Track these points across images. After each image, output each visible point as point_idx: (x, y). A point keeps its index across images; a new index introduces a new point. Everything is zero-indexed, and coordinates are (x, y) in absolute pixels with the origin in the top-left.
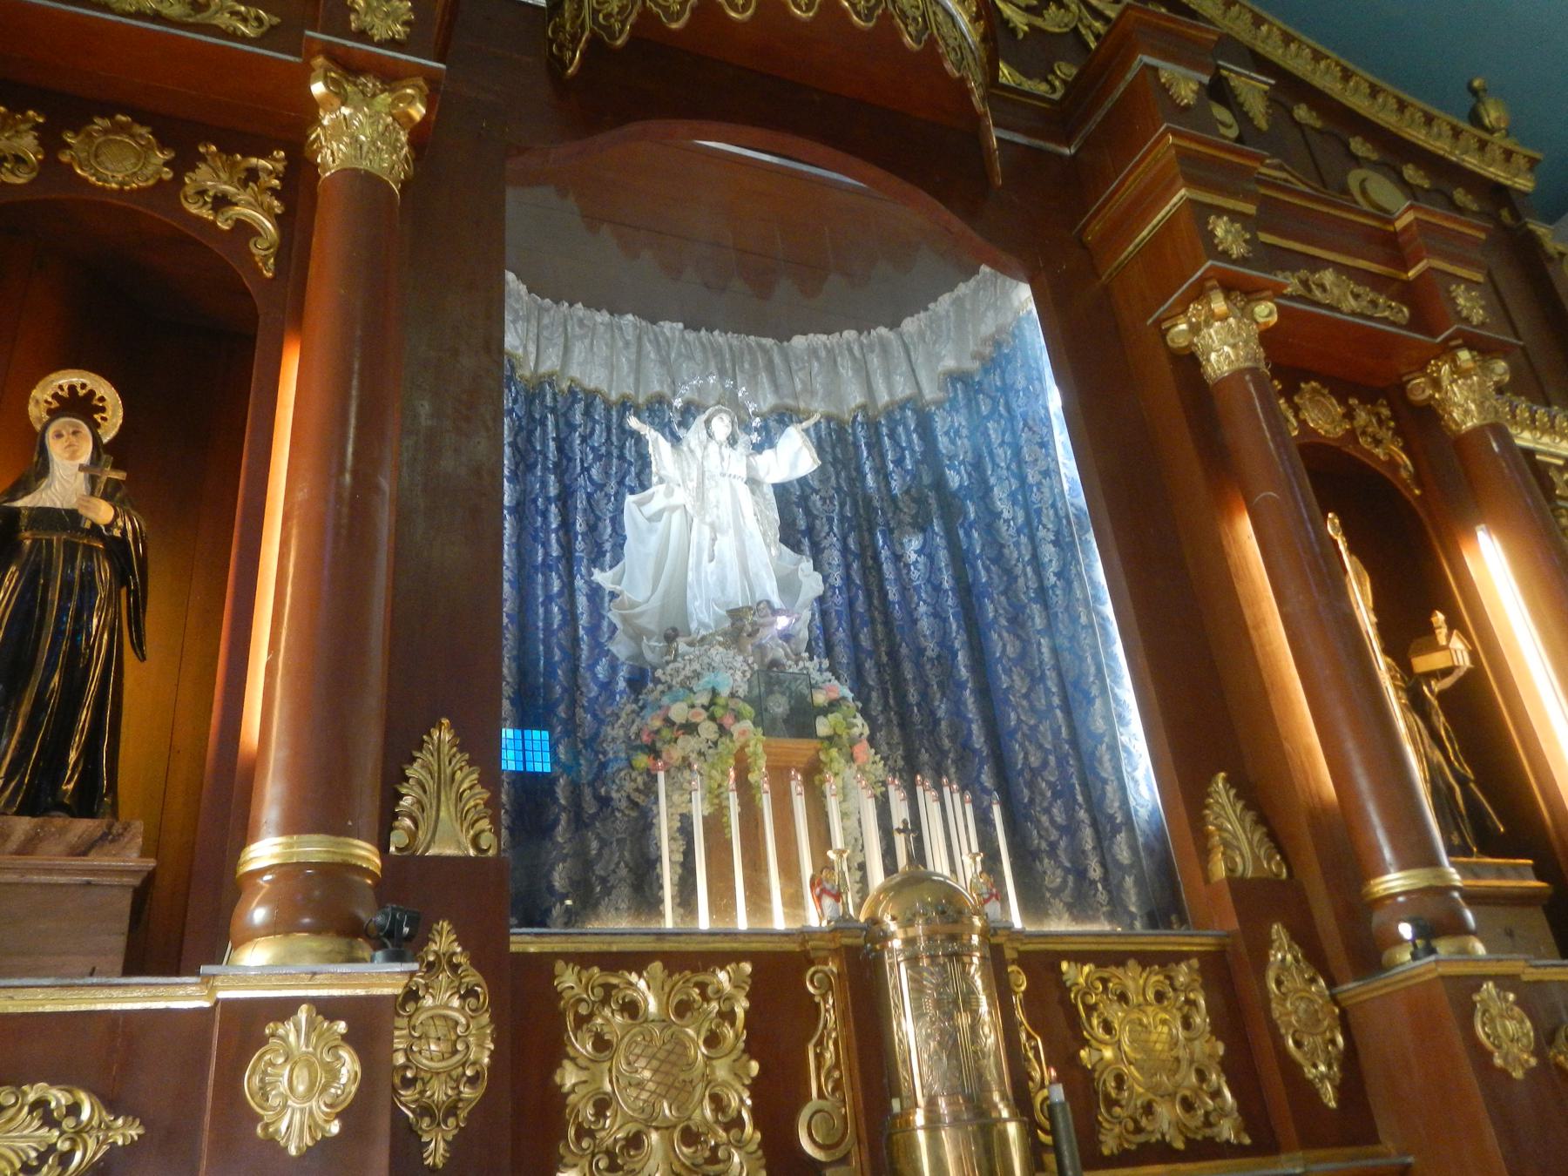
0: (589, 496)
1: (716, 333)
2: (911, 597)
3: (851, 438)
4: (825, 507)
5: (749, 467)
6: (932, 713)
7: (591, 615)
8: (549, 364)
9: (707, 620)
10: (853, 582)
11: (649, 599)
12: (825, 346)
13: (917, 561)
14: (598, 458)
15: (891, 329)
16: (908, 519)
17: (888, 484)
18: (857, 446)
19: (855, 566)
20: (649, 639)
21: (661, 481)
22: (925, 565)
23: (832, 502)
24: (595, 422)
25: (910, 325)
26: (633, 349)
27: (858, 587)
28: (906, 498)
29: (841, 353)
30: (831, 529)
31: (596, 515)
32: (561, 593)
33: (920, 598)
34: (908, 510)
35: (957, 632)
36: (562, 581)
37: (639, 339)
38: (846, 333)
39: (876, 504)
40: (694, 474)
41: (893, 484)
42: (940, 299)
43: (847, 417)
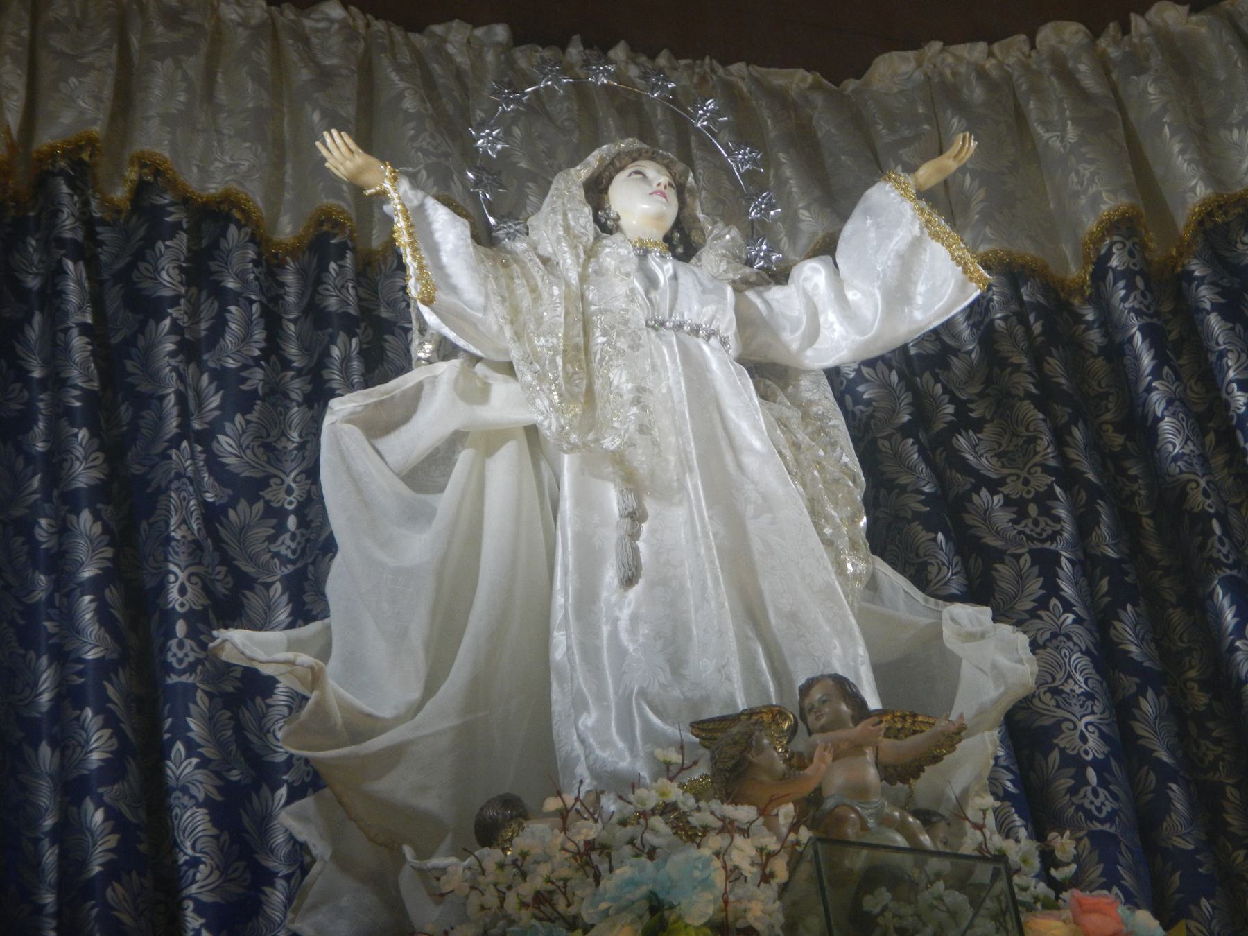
0: (212, 515)
1: (619, 52)
3: (1095, 336)
4: (1027, 526)
5: (747, 322)
7: (223, 868)
8: (67, 118)
9: (625, 764)
10: (1146, 756)
11: (419, 706)
12: (982, 74)
14: (241, 402)
15: (1195, 10)
18: (1117, 351)
19: (1148, 705)
20: (423, 854)
21: (446, 350)
23: (1046, 511)
24: (222, 296)
26: (349, 88)
27: (1166, 774)
30: (1054, 590)
31: (235, 572)
32: (113, 769)
36: (118, 733)
37: (367, 73)
38: (1047, 34)
39: (1199, 501)
40: (554, 310)
43: (1075, 271)
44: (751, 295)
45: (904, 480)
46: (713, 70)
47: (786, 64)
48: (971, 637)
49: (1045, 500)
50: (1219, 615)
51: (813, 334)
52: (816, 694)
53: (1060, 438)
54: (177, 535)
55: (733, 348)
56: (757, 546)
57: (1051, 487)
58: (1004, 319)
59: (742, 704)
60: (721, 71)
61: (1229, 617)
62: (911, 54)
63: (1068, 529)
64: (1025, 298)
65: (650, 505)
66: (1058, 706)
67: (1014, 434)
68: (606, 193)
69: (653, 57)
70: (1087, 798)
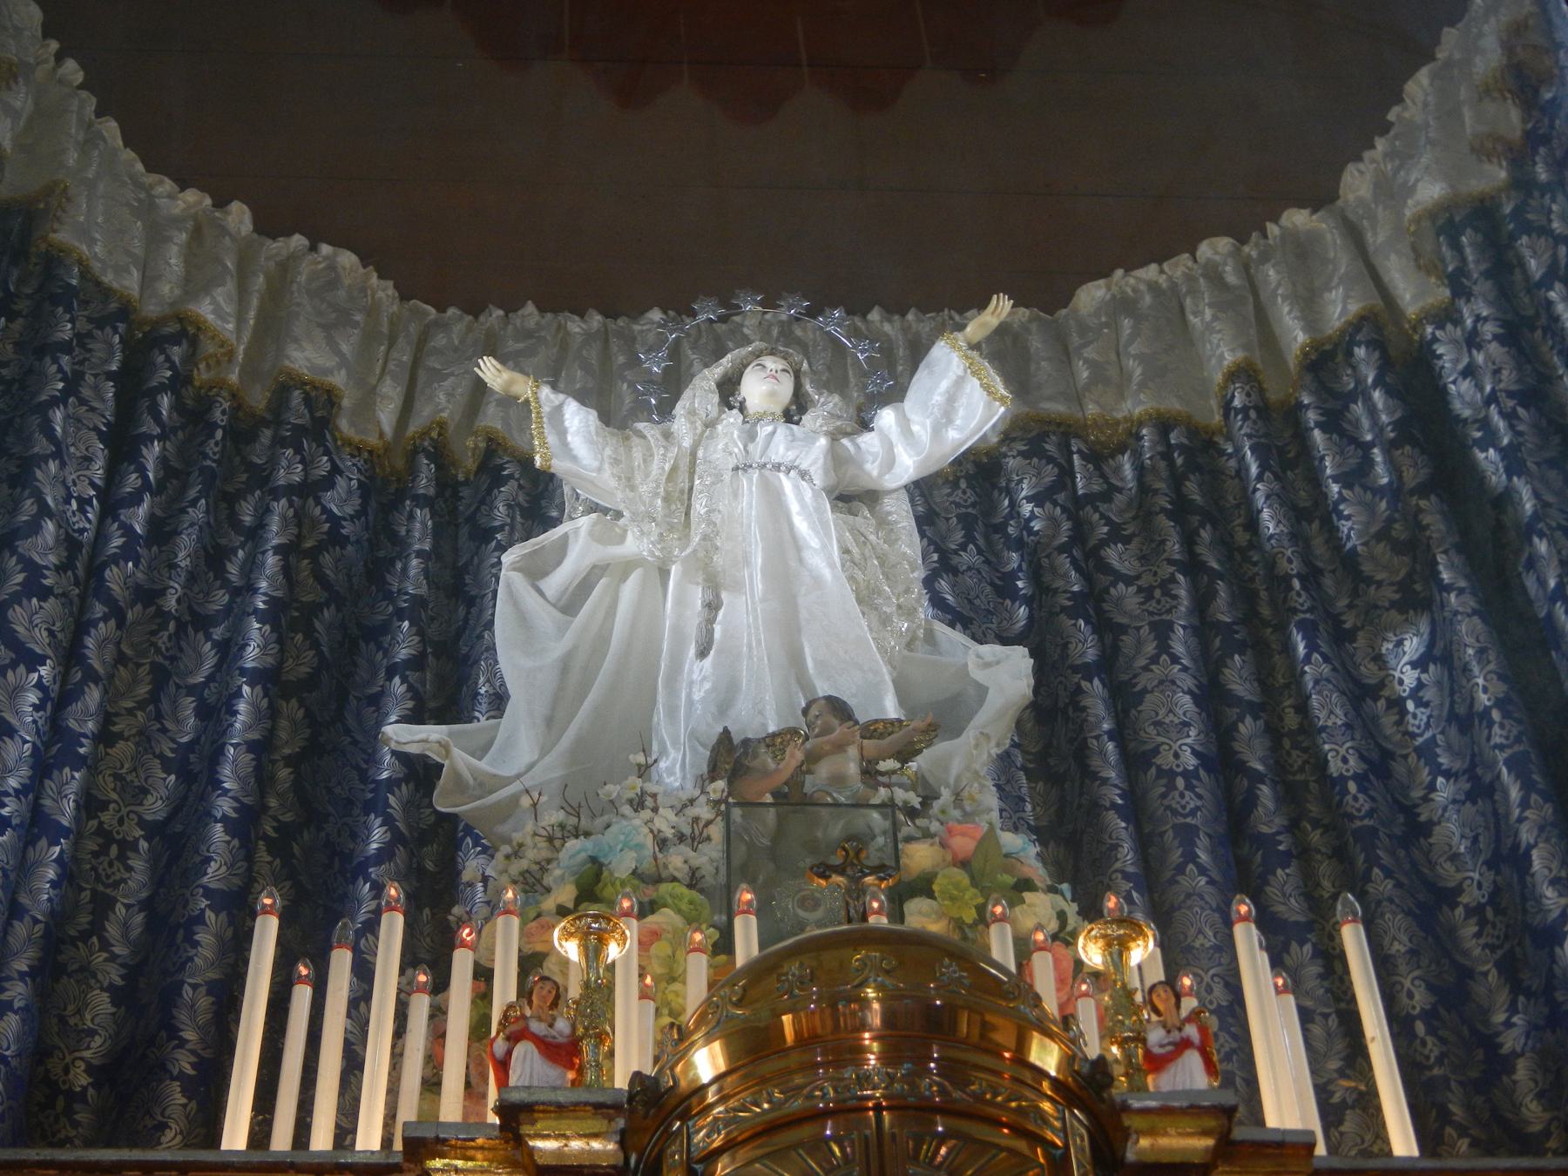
1: (875, 315)
2: (1411, 773)
4: (1153, 604)
5: (837, 460)
6: (1489, 1043)
10: (1242, 768)
12: (1153, 287)
13: (1420, 685)
15: (1315, 211)
16: (1389, 594)
17: (1331, 531)
19: (1247, 727)
22: (1439, 684)
25: (1356, 183)
28: (1380, 548)
29: (1194, 292)
30: (1164, 647)
33: (1437, 770)
34: (1385, 568)
35: (1525, 804)
38: (1205, 250)
41: (1345, 526)
42: (1410, 87)
44: (845, 441)
45: (1059, 583)
46: (951, 318)
48: (987, 665)
49: (1166, 585)
50: (1295, 649)
51: (890, 462)
52: (814, 711)
53: (1189, 540)
54: (482, 691)
56: (804, 614)
57: (1173, 574)
58: (1150, 458)
59: (772, 728)
60: (957, 317)
61: (1301, 649)
62: (1101, 282)
63: (1185, 603)
64: (1173, 442)
65: (725, 596)
66: (1158, 734)
67: (1152, 541)
68: (739, 384)
69: (903, 315)
70: (1174, 800)
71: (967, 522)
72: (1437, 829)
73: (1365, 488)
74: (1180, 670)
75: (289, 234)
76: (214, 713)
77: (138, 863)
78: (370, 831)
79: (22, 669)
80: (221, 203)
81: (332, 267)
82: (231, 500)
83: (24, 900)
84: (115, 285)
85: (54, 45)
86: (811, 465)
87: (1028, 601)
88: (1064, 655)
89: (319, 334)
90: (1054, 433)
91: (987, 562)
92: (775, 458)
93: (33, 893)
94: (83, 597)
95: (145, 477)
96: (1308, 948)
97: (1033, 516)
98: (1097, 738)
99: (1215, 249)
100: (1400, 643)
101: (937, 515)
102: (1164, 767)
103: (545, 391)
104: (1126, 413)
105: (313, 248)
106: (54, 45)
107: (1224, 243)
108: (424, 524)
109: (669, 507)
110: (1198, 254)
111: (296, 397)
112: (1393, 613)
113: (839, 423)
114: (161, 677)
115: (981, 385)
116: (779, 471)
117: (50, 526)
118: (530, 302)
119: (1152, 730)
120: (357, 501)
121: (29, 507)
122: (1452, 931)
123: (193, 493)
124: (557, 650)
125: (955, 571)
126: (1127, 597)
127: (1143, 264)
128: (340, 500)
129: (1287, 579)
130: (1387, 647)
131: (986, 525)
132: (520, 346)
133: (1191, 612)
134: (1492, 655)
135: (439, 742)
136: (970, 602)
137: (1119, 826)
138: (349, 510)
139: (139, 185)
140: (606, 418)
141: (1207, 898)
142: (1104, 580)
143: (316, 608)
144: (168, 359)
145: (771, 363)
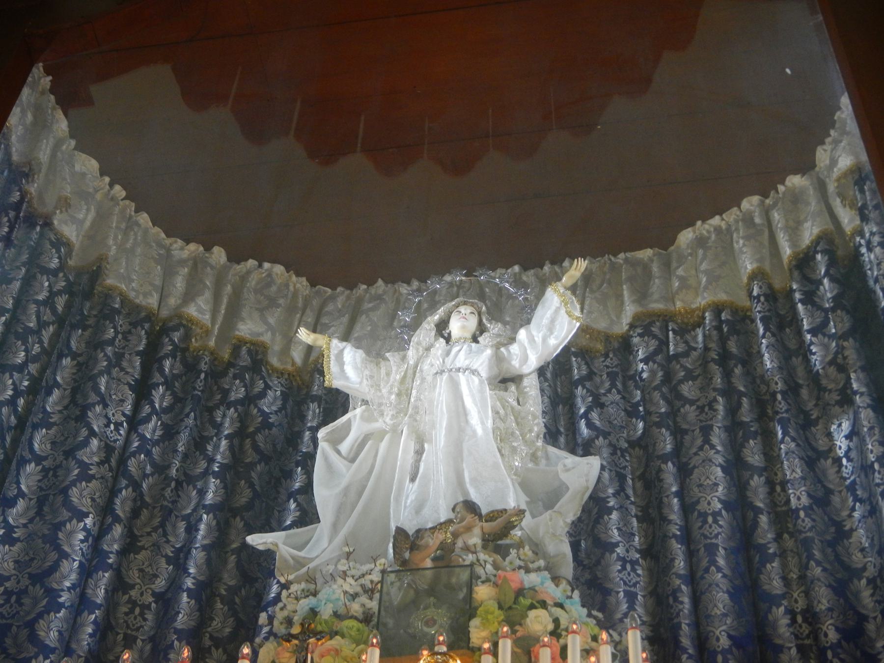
2: (844, 501)
5: (498, 359)
12: (718, 230)
13: (849, 449)
16: (835, 397)
17: (807, 361)
22: (857, 447)
23: (711, 408)
29: (737, 230)
30: (707, 441)
38: (745, 204)
44: (503, 349)
47: (640, 248)
49: (711, 405)
51: (525, 359)
52: (458, 509)
53: (727, 375)
55: (484, 374)
58: (708, 330)
59: (442, 520)
60: (613, 259)
62: (690, 229)
64: (723, 318)
65: (426, 446)
66: (700, 492)
67: (707, 378)
70: (706, 530)
71: (612, 376)
72: (855, 533)
73: (824, 335)
74: (715, 453)
75: (246, 260)
76: (192, 529)
77: (149, 616)
78: (270, 587)
79: (75, 521)
80: (208, 248)
81: (269, 275)
82: (211, 410)
83: (74, 646)
84: (144, 303)
85: (107, 179)
86: (479, 366)
87: (643, 419)
88: (654, 450)
89: (256, 315)
90: (658, 321)
91: (623, 398)
92: (458, 365)
93: (79, 641)
94: (115, 479)
95: (153, 407)
96: (782, 609)
97: (643, 371)
98: (667, 496)
99: (750, 203)
100: (840, 425)
101: (595, 374)
102: (702, 511)
103: (335, 342)
104: (698, 305)
105: (260, 266)
106: (107, 179)
107: (756, 199)
108: (314, 412)
109: (400, 399)
110: (742, 207)
111: (244, 350)
112: (837, 407)
113: (498, 340)
114: (167, 513)
115: (566, 312)
116: (459, 372)
117: (95, 442)
118: (380, 280)
119: (696, 490)
120: (279, 403)
121: (84, 432)
122: (857, 594)
123: (187, 410)
124: (344, 483)
125: (602, 406)
126: (690, 411)
127: (712, 216)
128: (270, 403)
129: (774, 395)
130: (834, 427)
131: (624, 377)
132: (371, 305)
133: (724, 418)
134: (877, 431)
135: (272, 543)
136: (610, 422)
137: (677, 549)
138: (274, 408)
139: (160, 245)
140: (368, 353)
141: (721, 586)
142: (678, 403)
143: (252, 465)
144: (171, 340)
145: (465, 310)
